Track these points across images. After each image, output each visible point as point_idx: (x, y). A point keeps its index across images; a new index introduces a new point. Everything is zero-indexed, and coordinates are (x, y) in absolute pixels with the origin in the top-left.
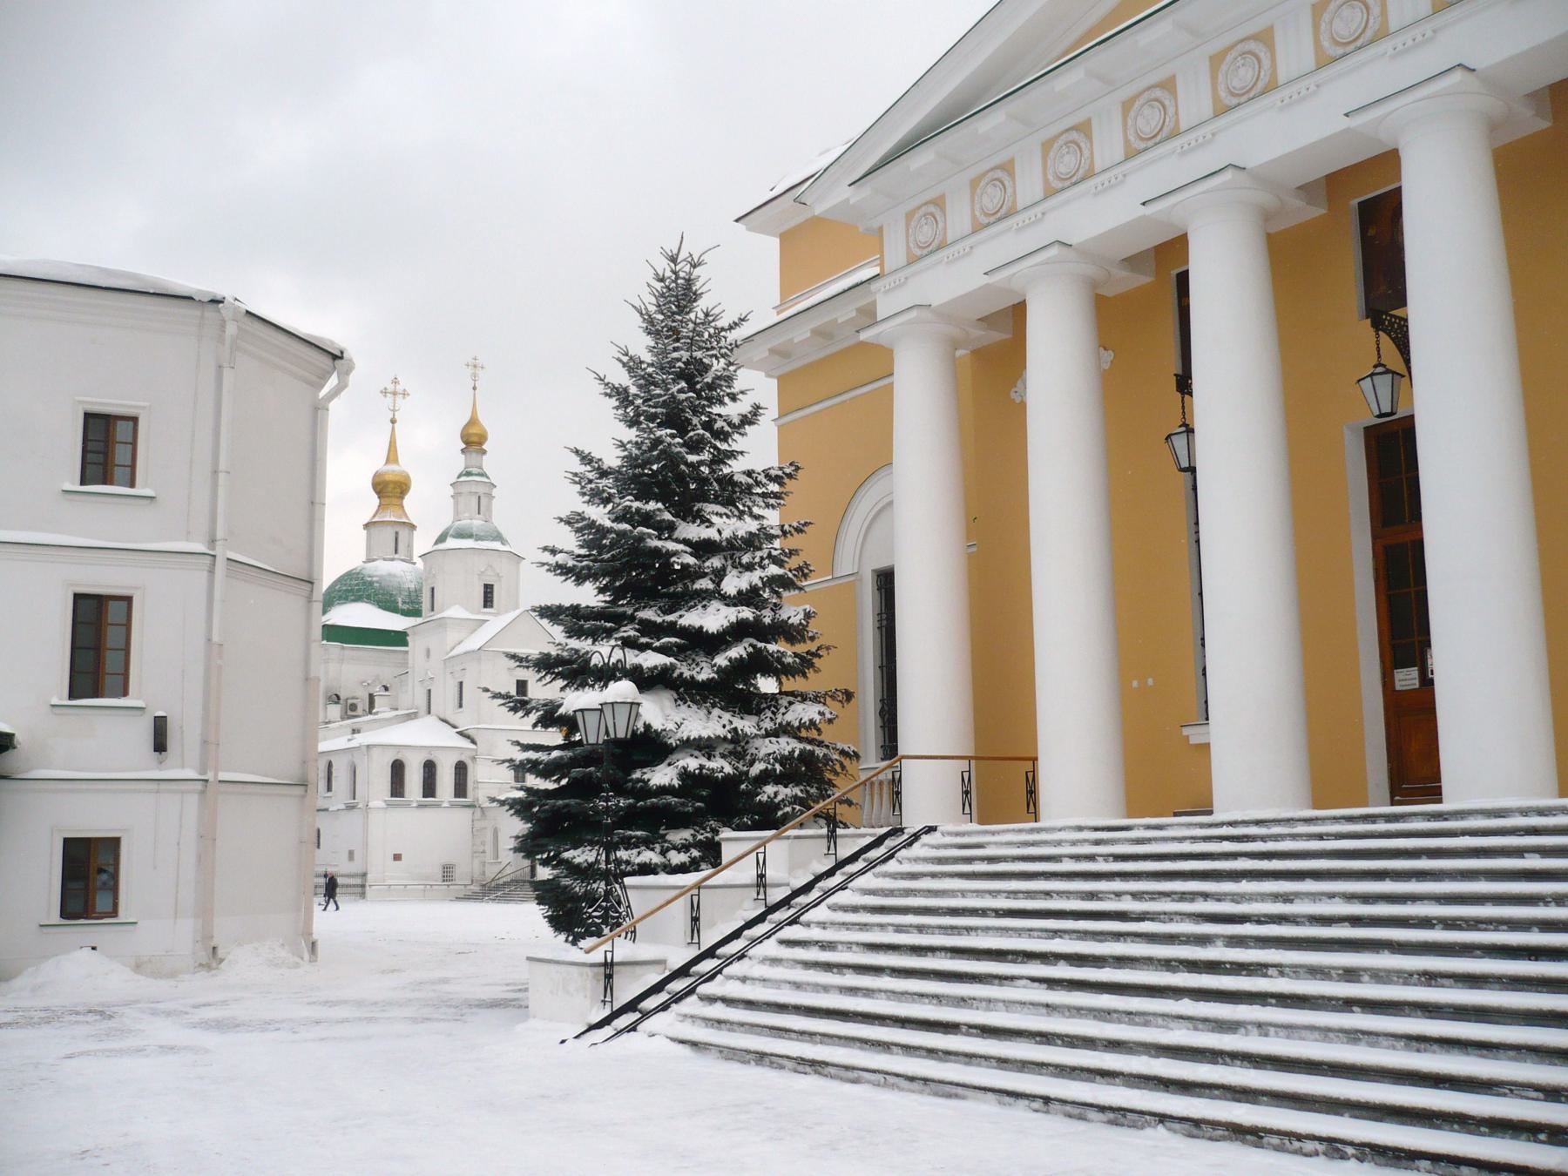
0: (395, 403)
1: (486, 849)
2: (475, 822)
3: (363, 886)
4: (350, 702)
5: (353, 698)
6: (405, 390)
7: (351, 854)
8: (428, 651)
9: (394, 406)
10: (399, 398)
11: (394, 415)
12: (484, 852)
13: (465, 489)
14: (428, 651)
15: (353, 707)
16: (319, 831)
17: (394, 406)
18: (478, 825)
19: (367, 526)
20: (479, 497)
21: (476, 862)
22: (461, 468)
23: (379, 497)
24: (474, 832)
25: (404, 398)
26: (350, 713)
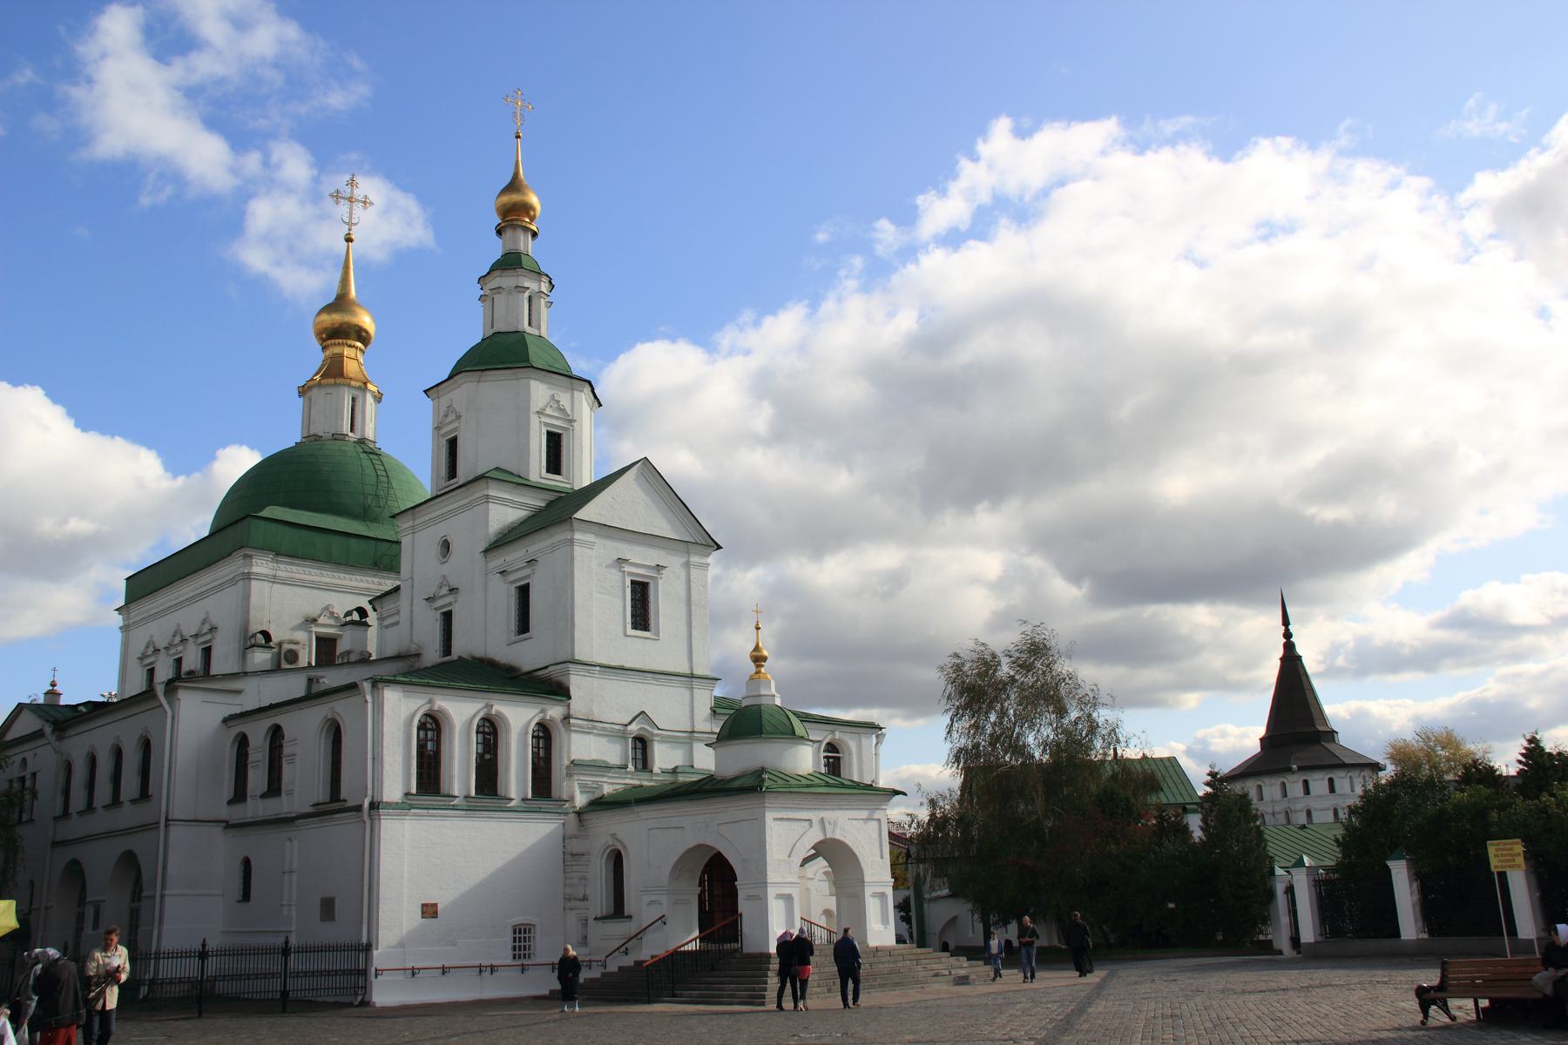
0: (351, 213)
1: (587, 893)
2: (566, 841)
3: (364, 973)
4: (286, 647)
5: (291, 642)
6: (366, 197)
7: (328, 908)
8: (446, 546)
9: (351, 218)
10: (358, 209)
11: (350, 230)
12: (585, 898)
13: (506, 280)
14: (446, 546)
15: (292, 656)
16: (247, 863)
17: (351, 218)
18: (576, 846)
19: (304, 391)
20: (530, 299)
21: (572, 918)
22: (497, 255)
23: (324, 348)
24: (571, 857)
25: (365, 208)
26: (285, 665)
